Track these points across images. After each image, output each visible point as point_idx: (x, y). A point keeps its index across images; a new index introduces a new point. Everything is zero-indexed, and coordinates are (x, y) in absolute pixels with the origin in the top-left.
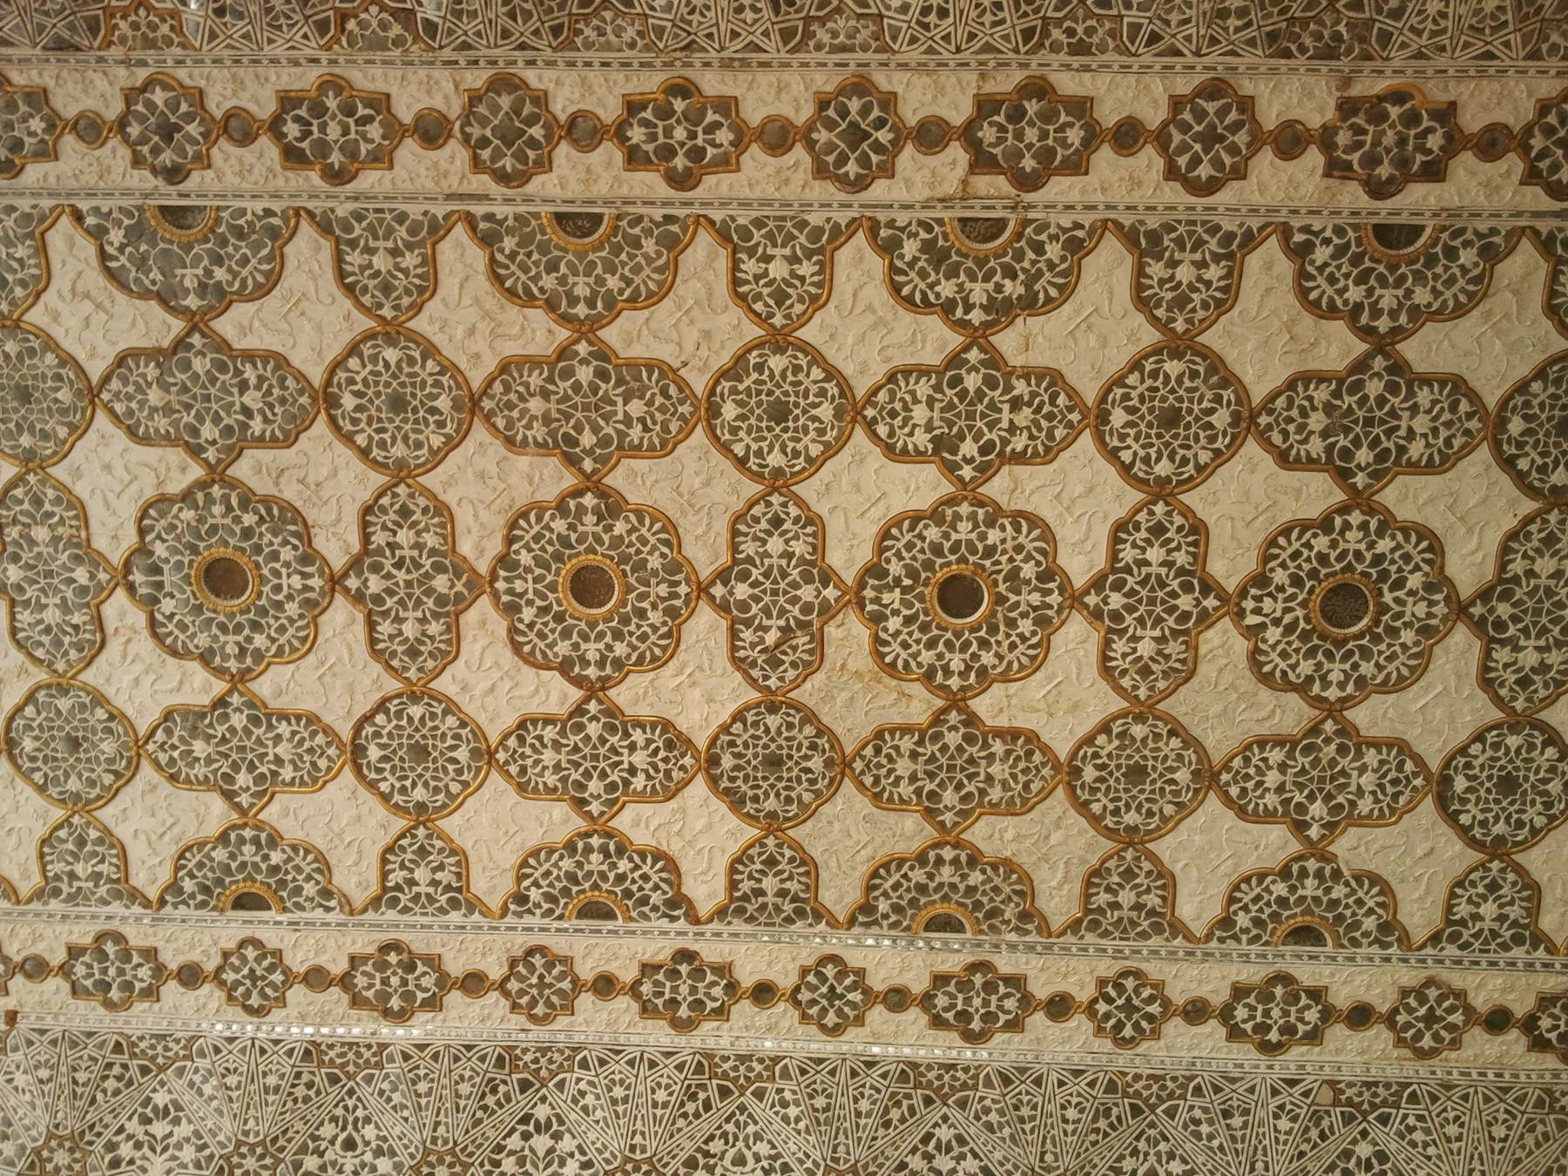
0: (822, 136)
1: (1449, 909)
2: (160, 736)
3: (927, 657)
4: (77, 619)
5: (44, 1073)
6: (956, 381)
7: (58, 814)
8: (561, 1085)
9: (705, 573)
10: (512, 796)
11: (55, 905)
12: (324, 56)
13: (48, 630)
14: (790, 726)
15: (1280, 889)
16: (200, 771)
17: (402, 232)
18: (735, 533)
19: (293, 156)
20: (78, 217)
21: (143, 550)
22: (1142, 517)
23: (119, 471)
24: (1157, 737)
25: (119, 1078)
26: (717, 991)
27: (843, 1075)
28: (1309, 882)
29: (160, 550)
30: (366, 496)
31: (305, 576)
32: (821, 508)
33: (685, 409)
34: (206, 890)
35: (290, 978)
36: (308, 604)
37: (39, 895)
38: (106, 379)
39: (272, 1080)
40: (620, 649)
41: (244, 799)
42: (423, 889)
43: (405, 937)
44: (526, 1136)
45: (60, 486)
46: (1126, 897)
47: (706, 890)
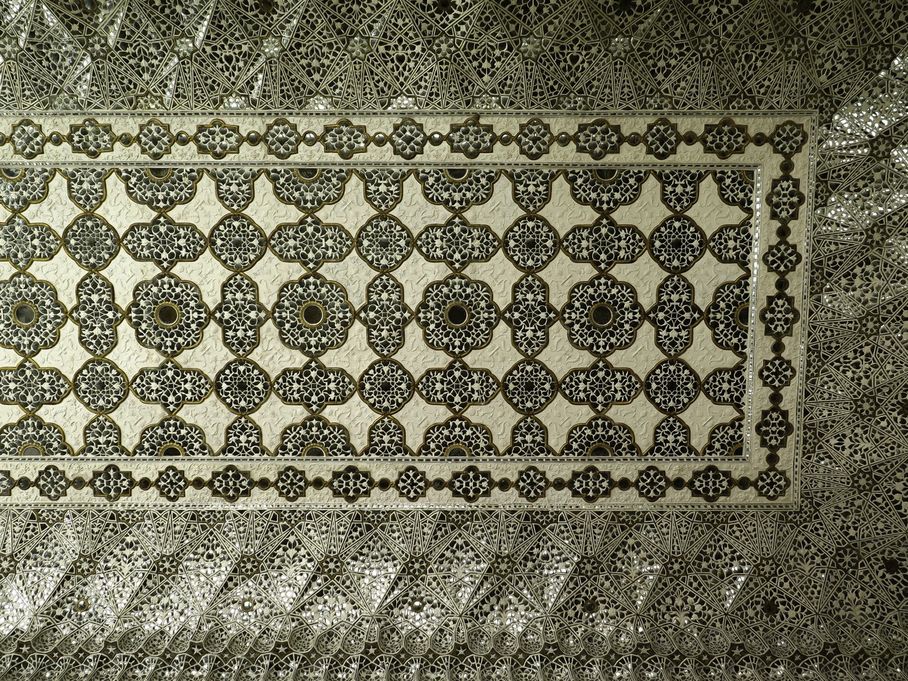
1: (655, 438)
2: (138, 381)
3: (446, 340)
4: (107, 332)
5: (79, 529)
6: (451, 230)
7: (93, 415)
8: (300, 527)
9: (357, 308)
10: (280, 403)
11: (89, 455)
12: (215, 111)
14: (393, 371)
15: (588, 432)
16: (154, 395)
18: (368, 291)
19: (202, 150)
21: (135, 304)
22: (524, 282)
23: (128, 272)
24: (536, 371)
25: (112, 530)
26: (365, 484)
27: (418, 517)
28: (600, 429)
29: (142, 303)
30: (224, 280)
31: (200, 313)
32: (402, 281)
33: (349, 243)
34: (153, 447)
35: (187, 483)
36: (200, 324)
37: (83, 451)
38: (125, 235)
39: (178, 528)
40: (324, 340)
42: (243, 444)
43: (235, 464)
44: (285, 550)
45: (104, 279)
46: (529, 438)
47: (359, 442)
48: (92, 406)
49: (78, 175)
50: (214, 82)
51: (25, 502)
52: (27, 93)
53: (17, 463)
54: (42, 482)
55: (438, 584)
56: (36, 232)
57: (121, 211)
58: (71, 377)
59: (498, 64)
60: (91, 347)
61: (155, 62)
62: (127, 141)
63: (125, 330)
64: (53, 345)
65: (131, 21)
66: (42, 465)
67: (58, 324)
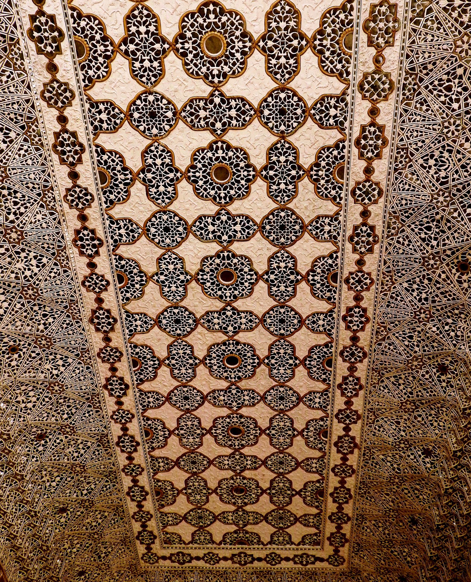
0: (348, 411)
2: (174, 256)
8: (80, 363)
13: (205, 226)
17: (329, 328)
19: (349, 309)
20: (336, 252)
21: (234, 256)
26: (118, 394)
29: (235, 261)
30: (255, 312)
33: (282, 381)
36: (221, 297)
38: (287, 252)
41: (156, 278)
42: (134, 323)
48: (149, 223)
49: (336, 223)
50: (396, 325)
51: (57, 176)
52: (404, 202)
53: (91, 170)
54: (78, 190)
55: (59, 443)
56: (290, 187)
57: (306, 251)
58: (171, 208)
59: (389, 464)
60: (198, 223)
61: (415, 294)
62: (360, 263)
63: (214, 248)
64: (198, 195)
65: (446, 292)
66: (92, 189)
67: (215, 198)
